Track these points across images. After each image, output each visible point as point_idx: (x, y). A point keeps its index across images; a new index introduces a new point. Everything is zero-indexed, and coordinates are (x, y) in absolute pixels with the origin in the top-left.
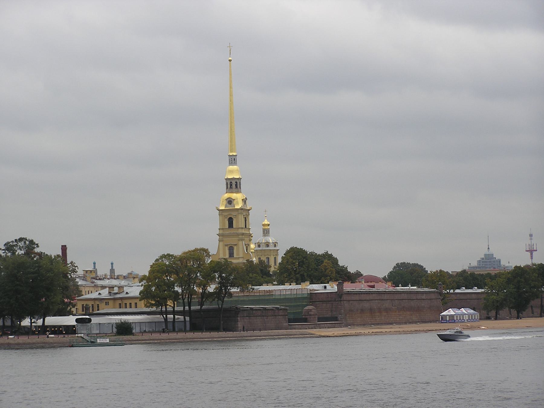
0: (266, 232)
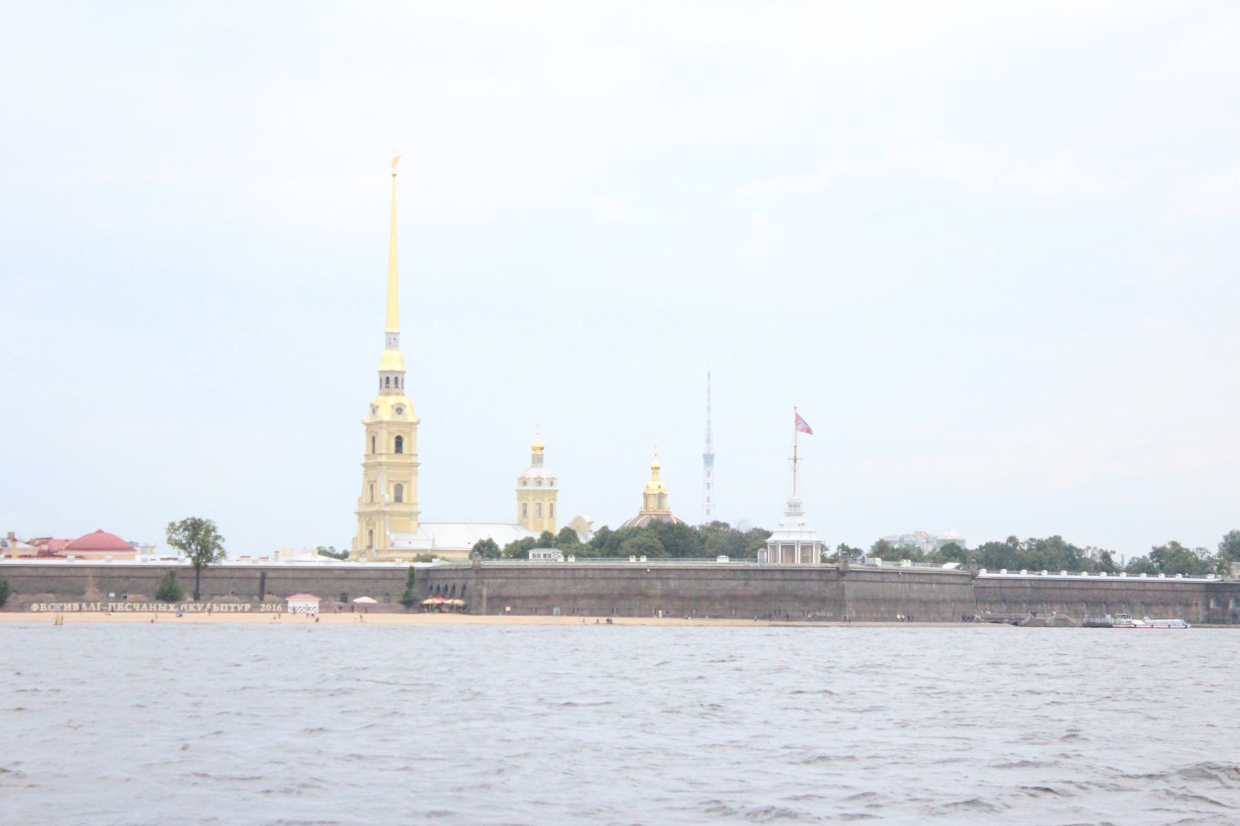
0: (538, 460)
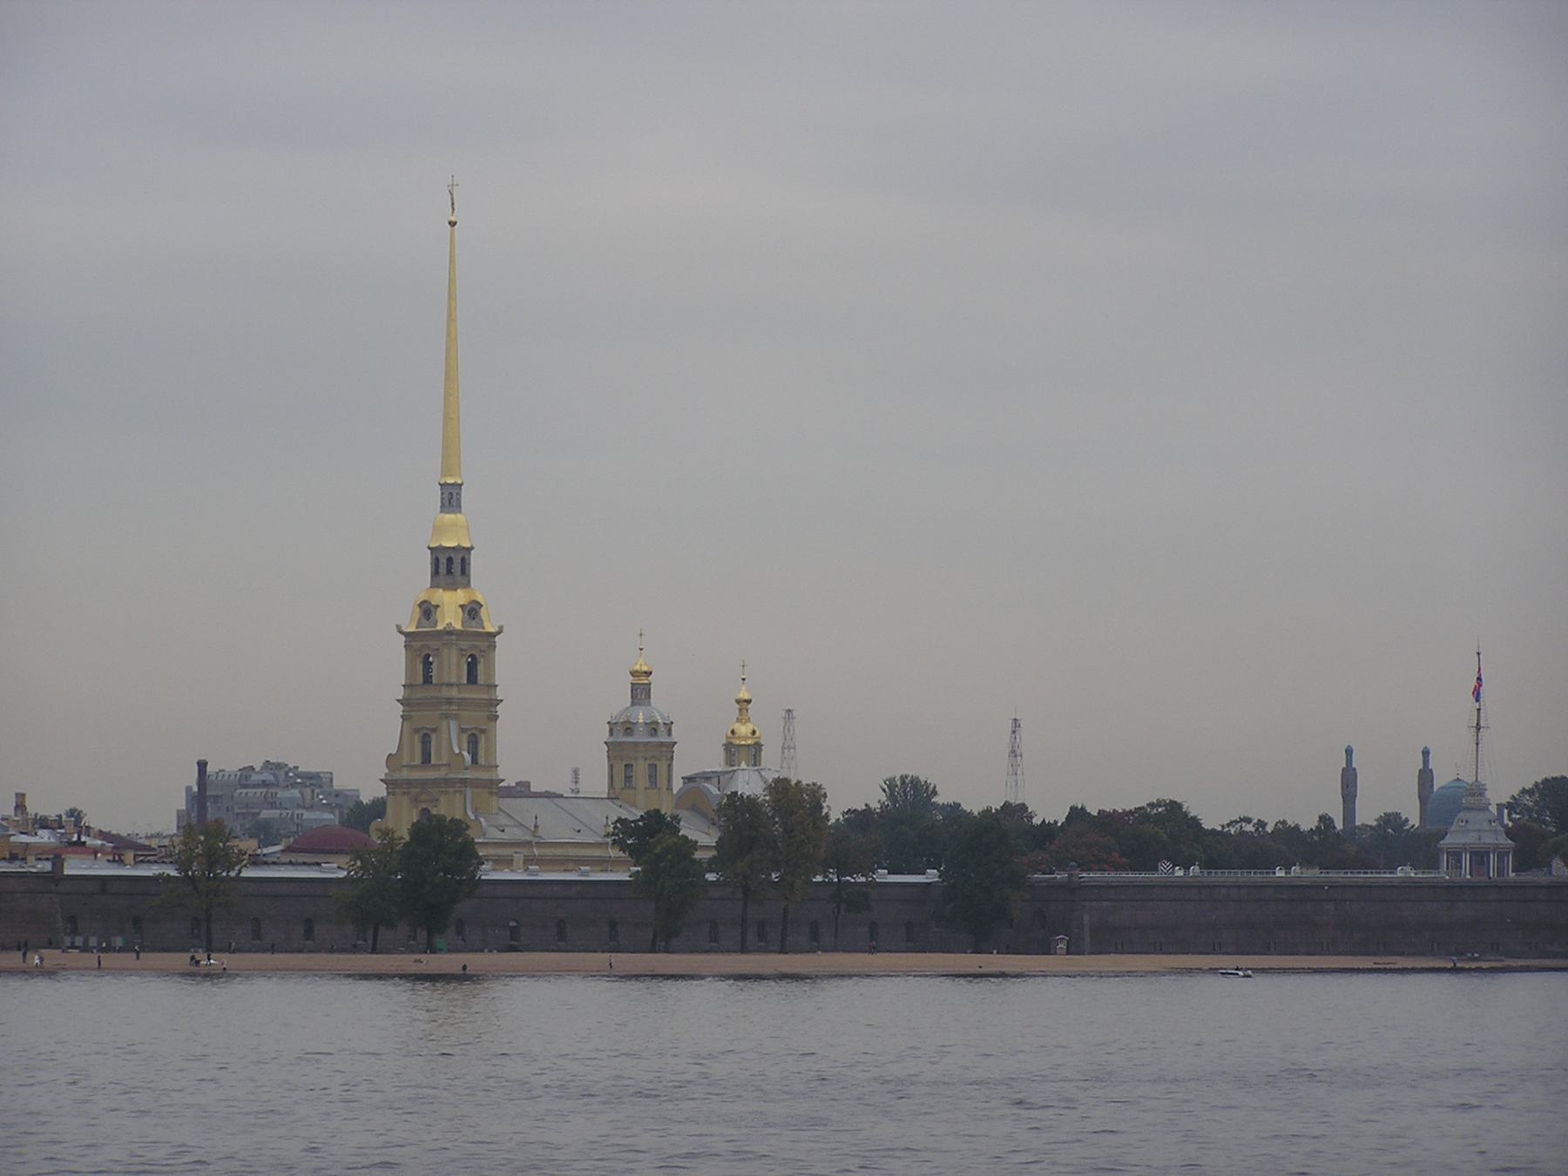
0: (640, 692)
